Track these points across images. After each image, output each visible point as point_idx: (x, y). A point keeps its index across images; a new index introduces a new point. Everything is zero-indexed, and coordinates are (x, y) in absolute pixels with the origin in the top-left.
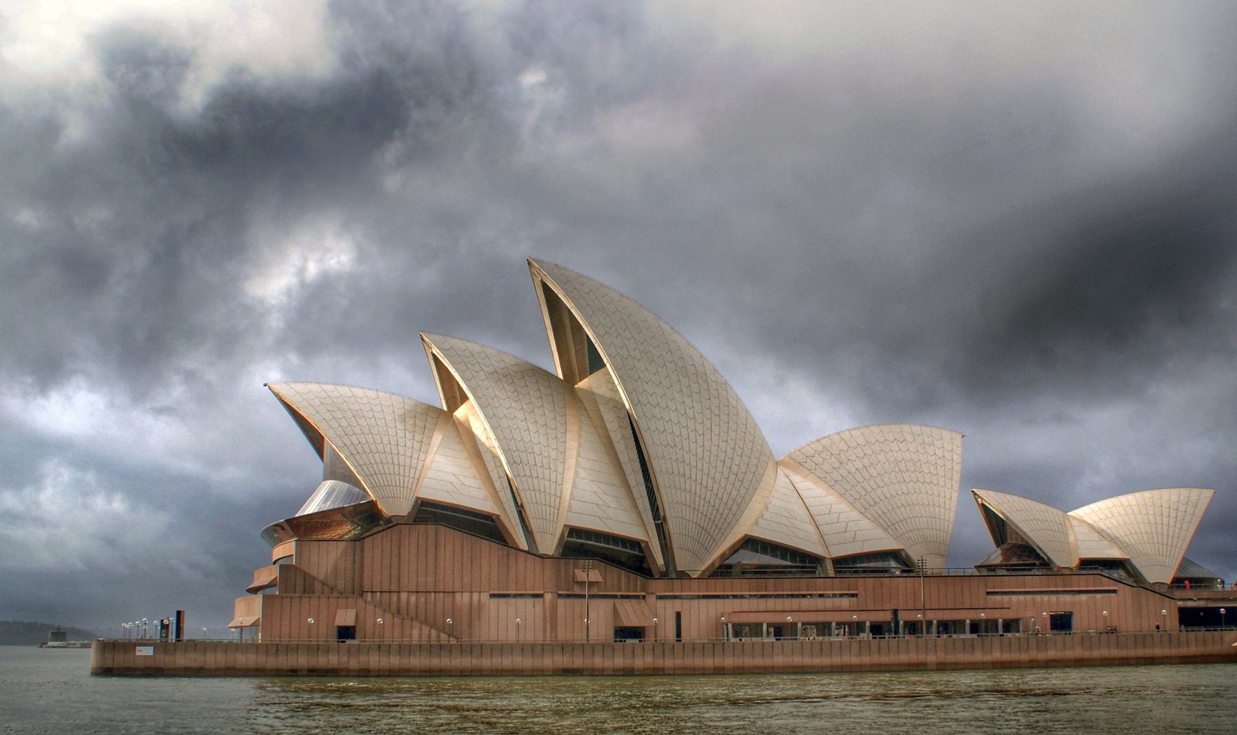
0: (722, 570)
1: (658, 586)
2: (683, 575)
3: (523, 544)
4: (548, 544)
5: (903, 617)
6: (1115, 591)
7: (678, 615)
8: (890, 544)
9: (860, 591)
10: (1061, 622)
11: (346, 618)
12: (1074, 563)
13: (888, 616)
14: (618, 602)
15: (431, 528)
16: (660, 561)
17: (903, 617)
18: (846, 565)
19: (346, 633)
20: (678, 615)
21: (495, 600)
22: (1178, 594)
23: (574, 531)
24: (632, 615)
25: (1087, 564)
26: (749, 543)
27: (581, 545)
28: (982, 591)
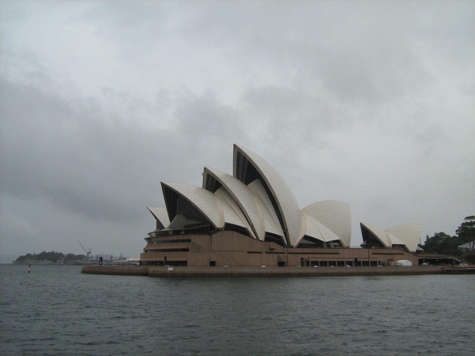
0: (300, 246)
2: (292, 247)
3: (255, 238)
4: (262, 237)
6: (403, 254)
8: (337, 238)
9: (340, 253)
12: (391, 246)
14: (280, 255)
15: (231, 232)
16: (286, 243)
19: (213, 264)
21: (249, 254)
22: (418, 255)
23: (267, 234)
25: (394, 246)
26: (306, 237)
27: (270, 237)
28: (371, 252)
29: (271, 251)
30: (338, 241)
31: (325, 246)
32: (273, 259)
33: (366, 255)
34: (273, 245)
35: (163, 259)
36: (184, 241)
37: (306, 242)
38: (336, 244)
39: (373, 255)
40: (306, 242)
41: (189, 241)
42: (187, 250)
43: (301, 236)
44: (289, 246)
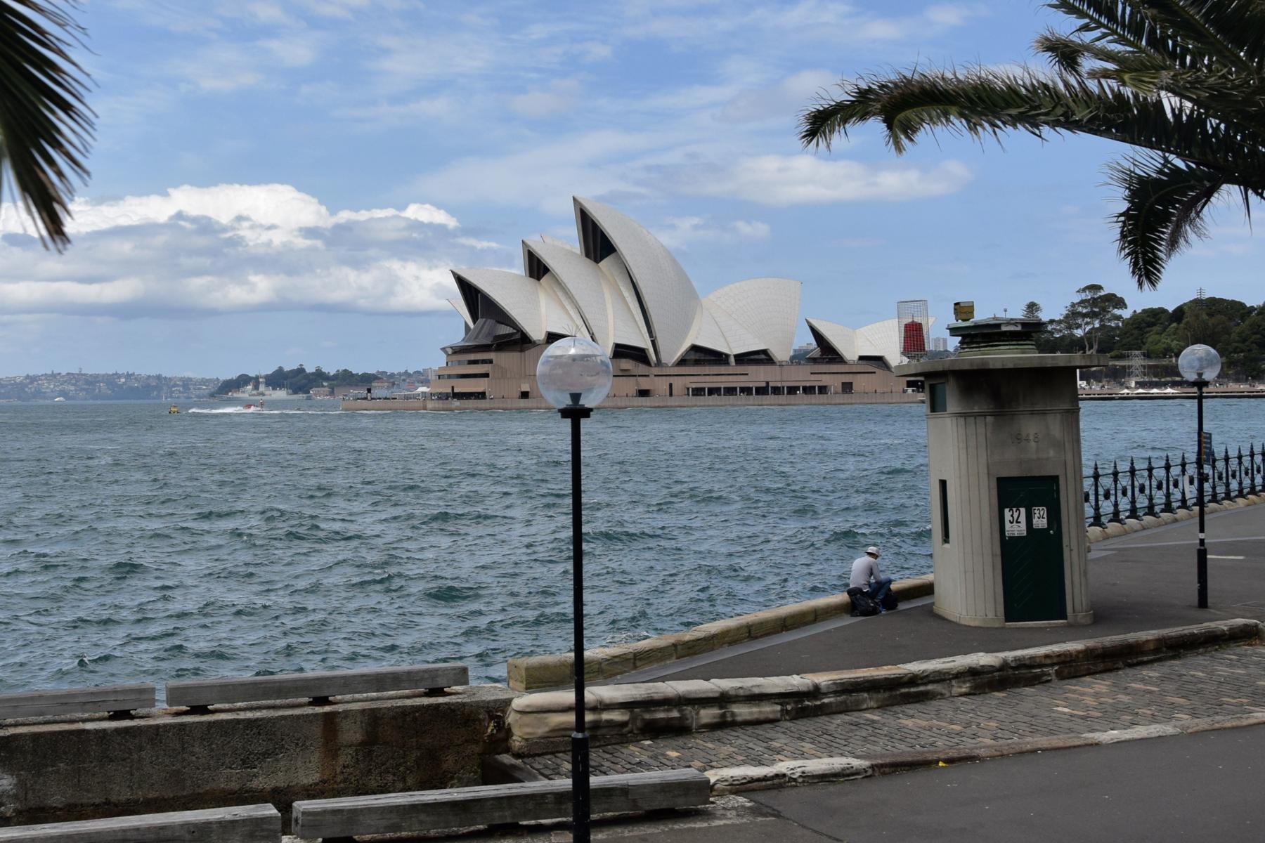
0: (682, 362)
1: (656, 371)
5: (771, 384)
7: (671, 385)
10: (847, 387)
11: (525, 388)
12: (856, 358)
13: (764, 385)
16: (654, 358)
17: (771, 384)
18: (743, 359)
20: (671, 385)
23: (617, 346)
24: (645, 384)
26: (695, 348)
27: (621, 351)
29: (625, 374)
30: (765, 352)
31: (732, 360)
32: (630, 386)
33: (803, 375)
34: (626, 364)
35: (449, 390)
36: (484, 362)
37: (693, 356)
38: (763, 356)
39: (813, 377)
40: (693, 356)
41: (491, 362)
42: (486, 375)
43: (686, 345)
44: (659, 363)
